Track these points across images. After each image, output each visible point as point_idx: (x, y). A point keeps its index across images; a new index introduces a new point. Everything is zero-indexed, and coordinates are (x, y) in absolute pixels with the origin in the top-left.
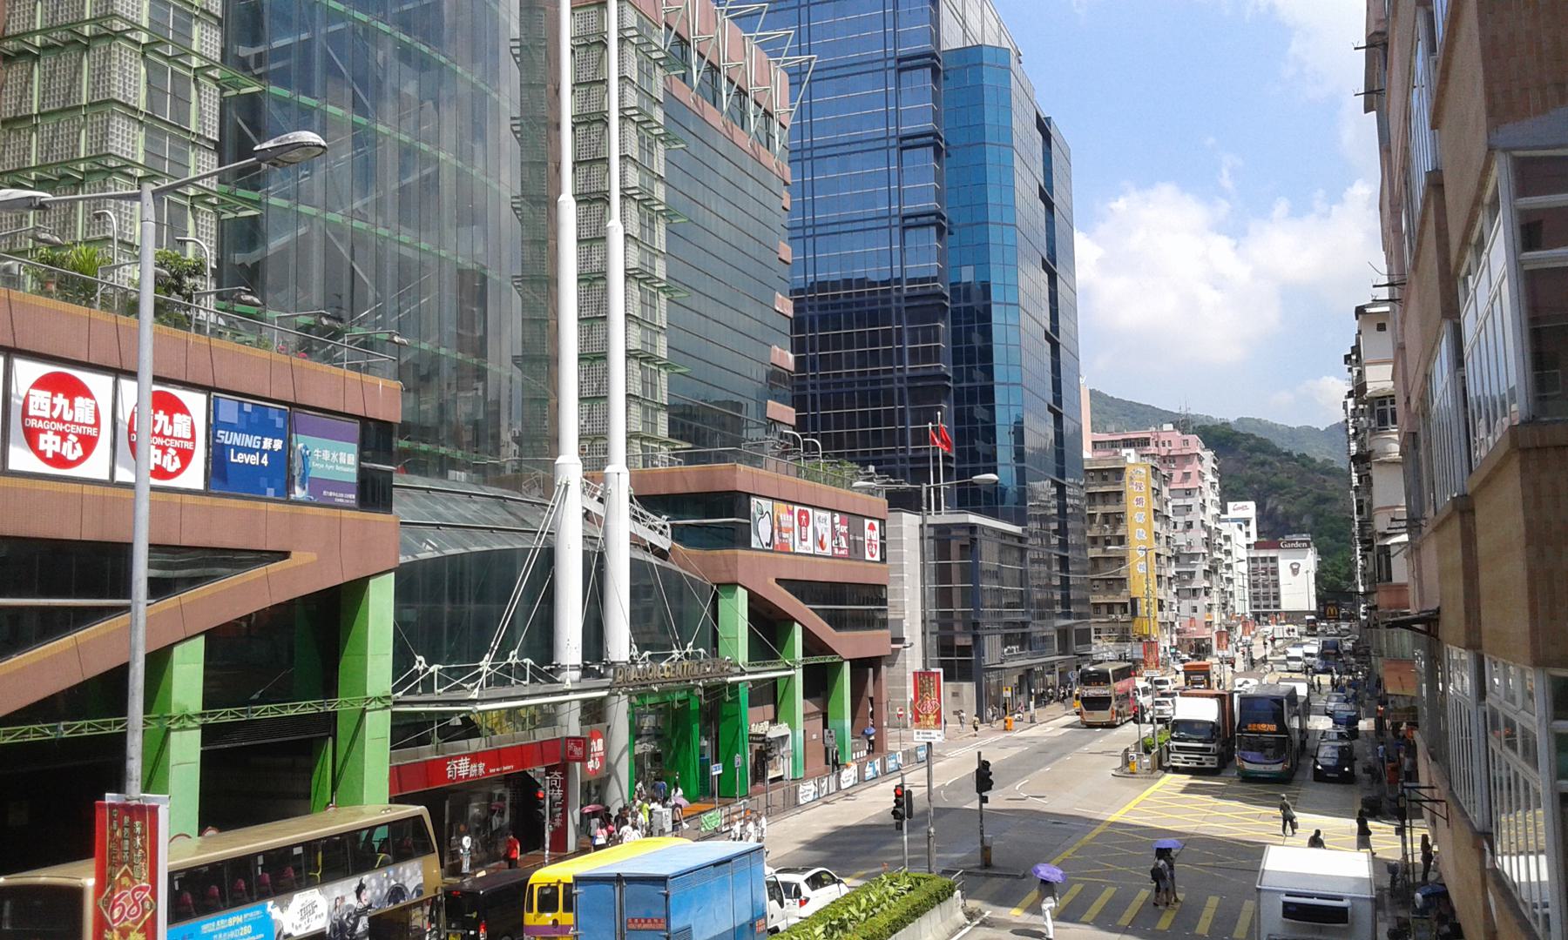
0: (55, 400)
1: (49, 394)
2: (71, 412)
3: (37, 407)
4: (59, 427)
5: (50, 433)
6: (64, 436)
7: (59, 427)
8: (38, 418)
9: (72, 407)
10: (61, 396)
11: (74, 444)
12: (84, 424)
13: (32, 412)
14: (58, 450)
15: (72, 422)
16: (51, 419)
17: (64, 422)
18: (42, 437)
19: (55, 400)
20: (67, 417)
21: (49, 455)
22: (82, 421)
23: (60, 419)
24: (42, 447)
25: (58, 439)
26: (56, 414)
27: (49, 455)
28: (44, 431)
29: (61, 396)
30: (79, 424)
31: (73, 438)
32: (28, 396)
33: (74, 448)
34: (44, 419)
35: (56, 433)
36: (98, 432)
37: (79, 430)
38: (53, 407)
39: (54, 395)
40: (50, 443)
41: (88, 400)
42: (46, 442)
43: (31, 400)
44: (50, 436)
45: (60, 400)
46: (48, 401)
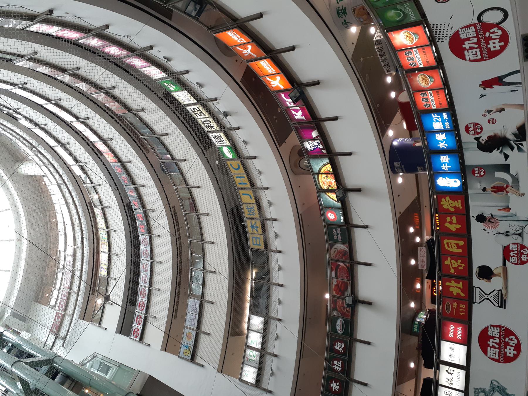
0: (468, 48)
1: (466, 52)
4: (483, 43)
5: (489, 46)
7: (483, 43)
8: (482, 54)
9: (468, 39)
10: (464, 46)
14: (498, 40)
19: (468, 48)
20: (475, 40)
21: (502, 44)
22: (475, 33)
25: (491, 42)
26: (476, 46)
27: (502, 44)
30: (477, 33)
31: (487, 34)
39: (465, 49)
42: (495, 47)
44: (491, 46)
46: (469, 51)
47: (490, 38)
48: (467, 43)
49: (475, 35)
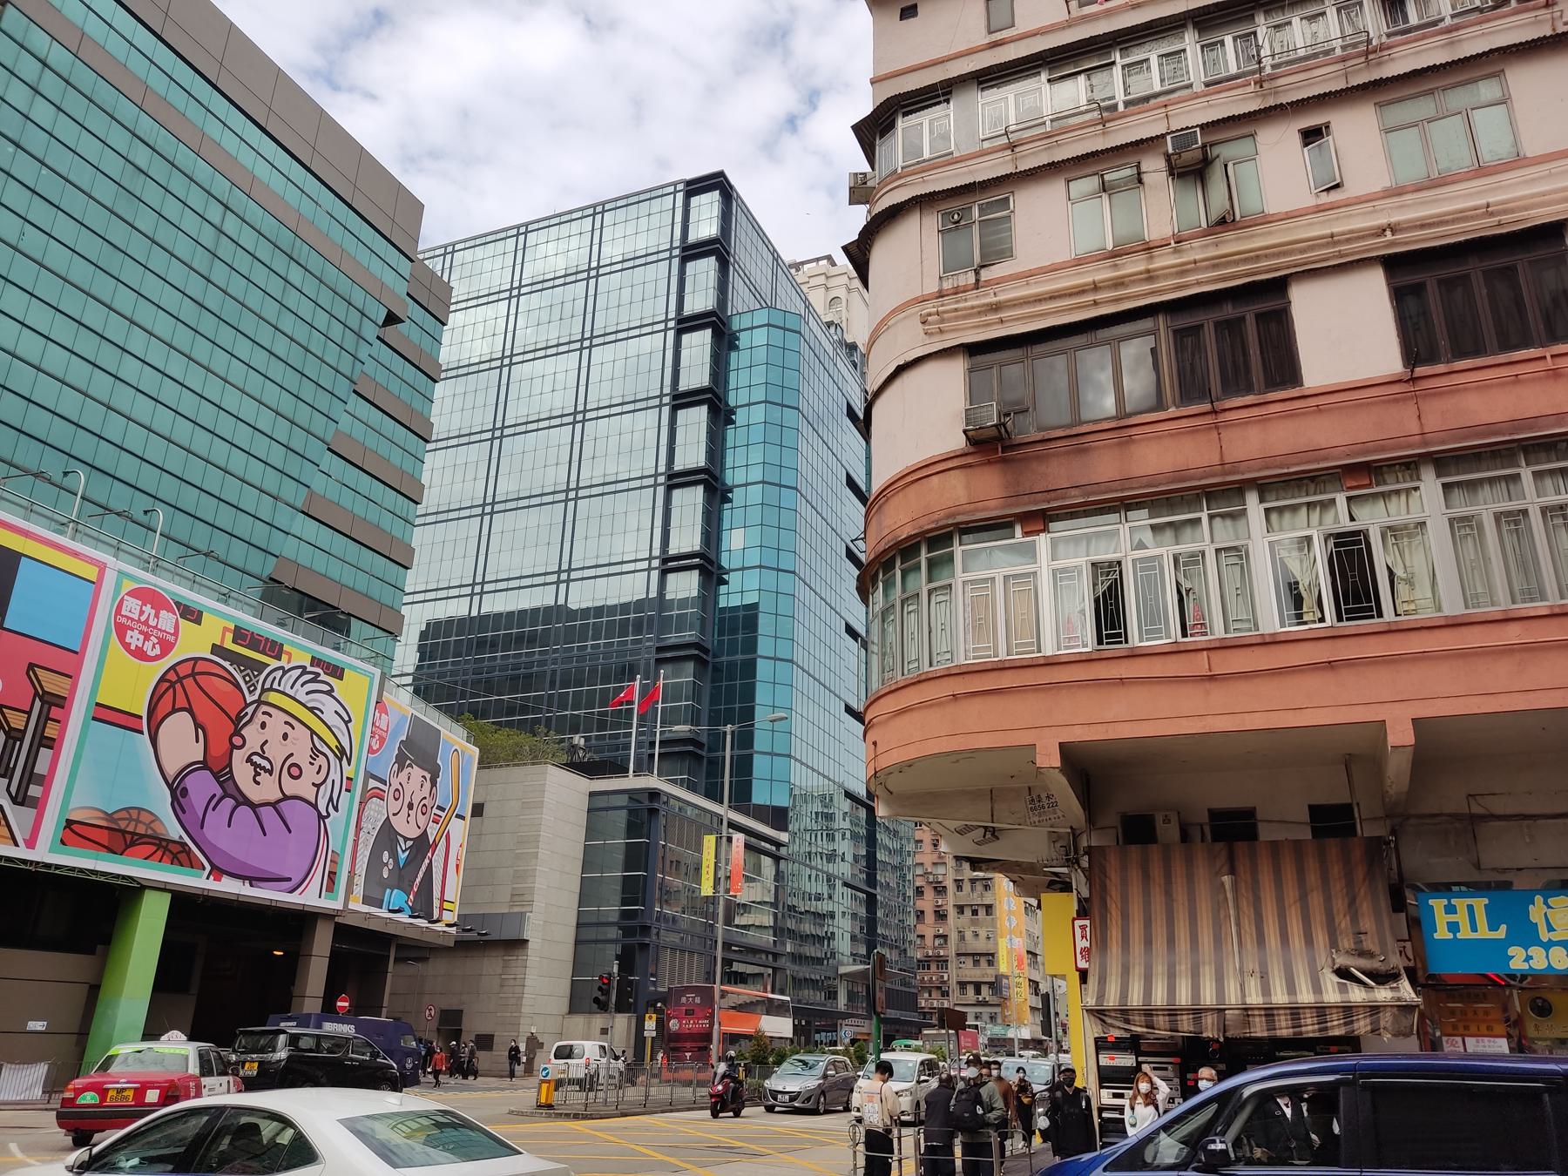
0: (144, 608)
1: (140, 603)
3: (128, 609)
4: (145, 629)
6: (147, 637)
7: (145, 629)
8: (128, 618)
9: (157, 616)
10: (149, 606)
11: (154, 645)
12: (165, 631)
15: (156, 627)
16: (139, 621)
17: (149, 626)
18: (129, 633)
19: (144, 608)
20: (152, 622)
21: (133, 647)
23: (146, 623)
24: (128, 640)
25: (142, 637)
26: (143, 618)
27: (133, 647)
28: (132, 629)
29: (149, 606)
30: (160, 630)
32: (122, 599)
33: (154, 647)
34: (132, 620)
35: (141, 632)
36: (176, 640)
37: (160, 635)
38: (142, 612)
39: (144, 604)
45: (148, 609)
48: (153, 612)
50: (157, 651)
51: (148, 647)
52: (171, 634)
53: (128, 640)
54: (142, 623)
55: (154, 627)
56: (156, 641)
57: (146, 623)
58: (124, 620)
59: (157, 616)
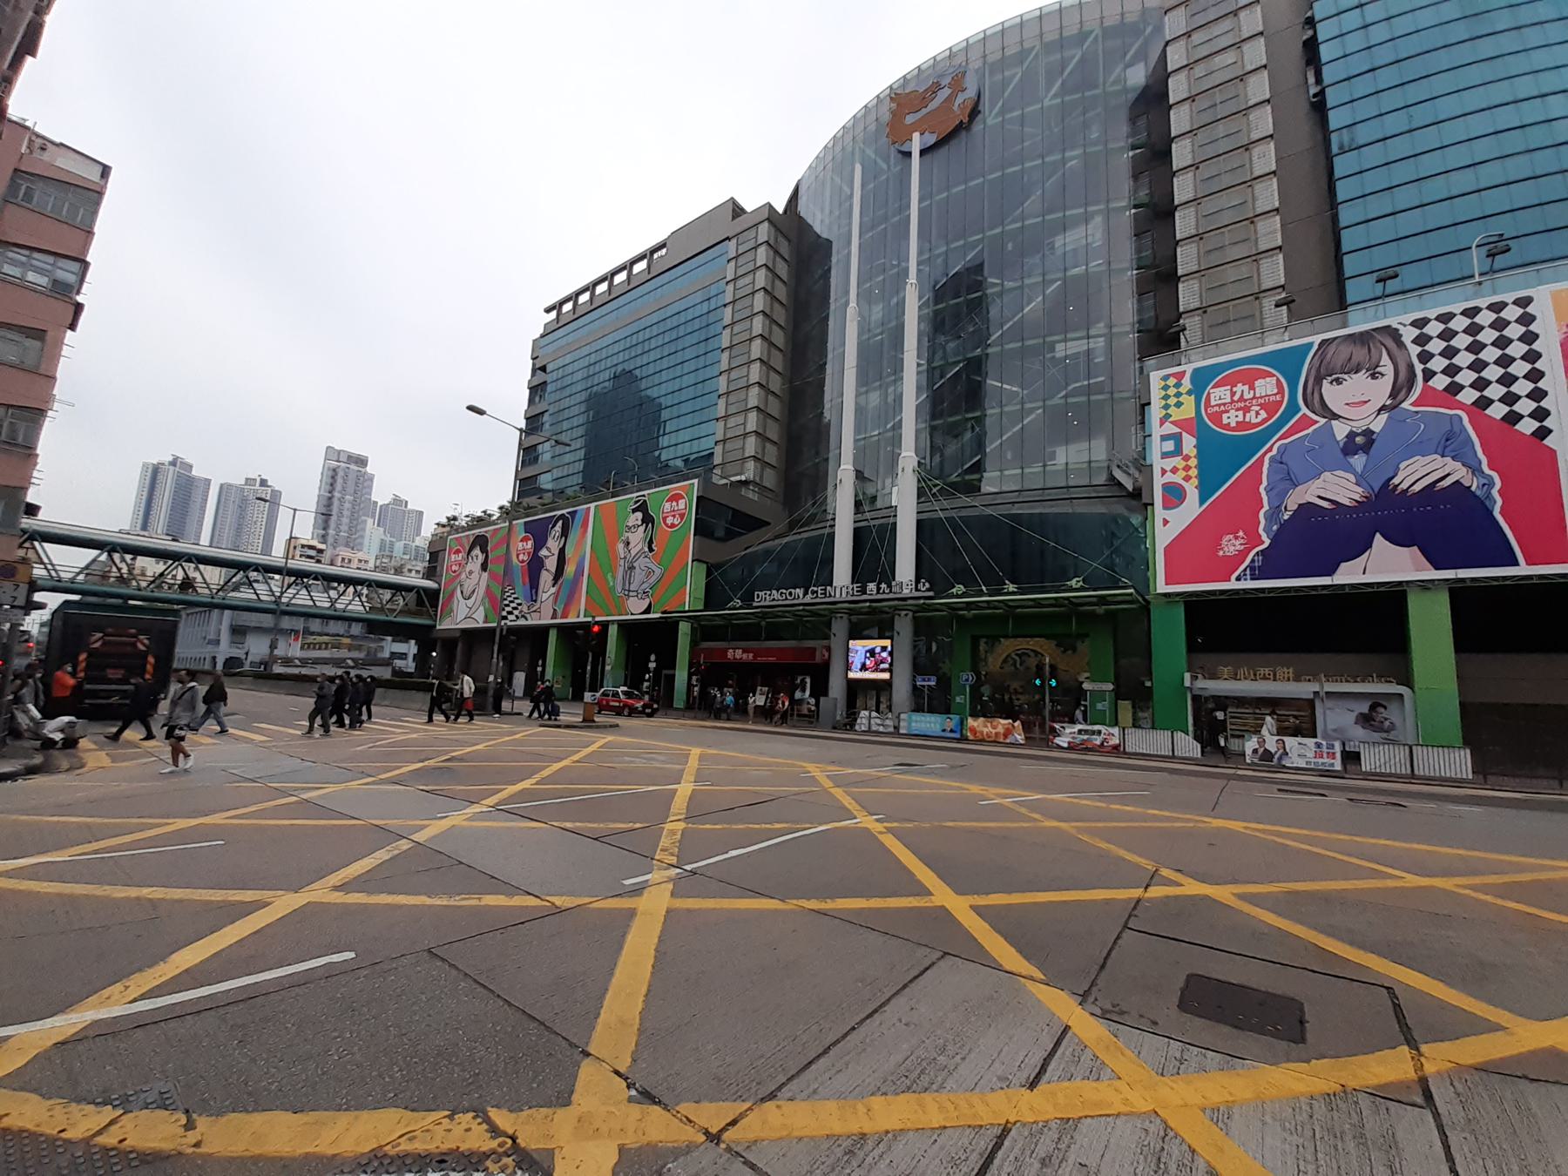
0: (1234, 389)
1: (1229, 387)
2: (1252, 392)
8: (1219, 405)
9: (1252, 388)
13: (1213, 403)
14: (1240, 418)
15: (1254, 397)
16: (1233, 401)
17: (1246, 400)
18: (1225, 416)
21: (1233, 424)
22: (1263, 394)
23: (1242, 399)
24: (1225, 421)
25: (1240, 413)
27: (1233, 424)
28: (1227, 412)
29: (1240, 385)
30: (1261, 397)
33: (1257, 413)
34: (1224, 404)
35: (1237, 410)
38: (1233, 394)
40: (1233, 417)
41: (1268, 379)
43: (1212, 396)
46: (1228, 393)
47: (1246, 410)
48: (1246, 388)
49: (1258, 395)
50: (1263, 415)
51: (1251, 417)
52: (1275, 395)
53: (1225, 421)
54: (1237, 402)
55: (1252, 399)
56: (1258, 408)
57: (1242, 399)
58: (1217, 409)
59: (1252, 388)
